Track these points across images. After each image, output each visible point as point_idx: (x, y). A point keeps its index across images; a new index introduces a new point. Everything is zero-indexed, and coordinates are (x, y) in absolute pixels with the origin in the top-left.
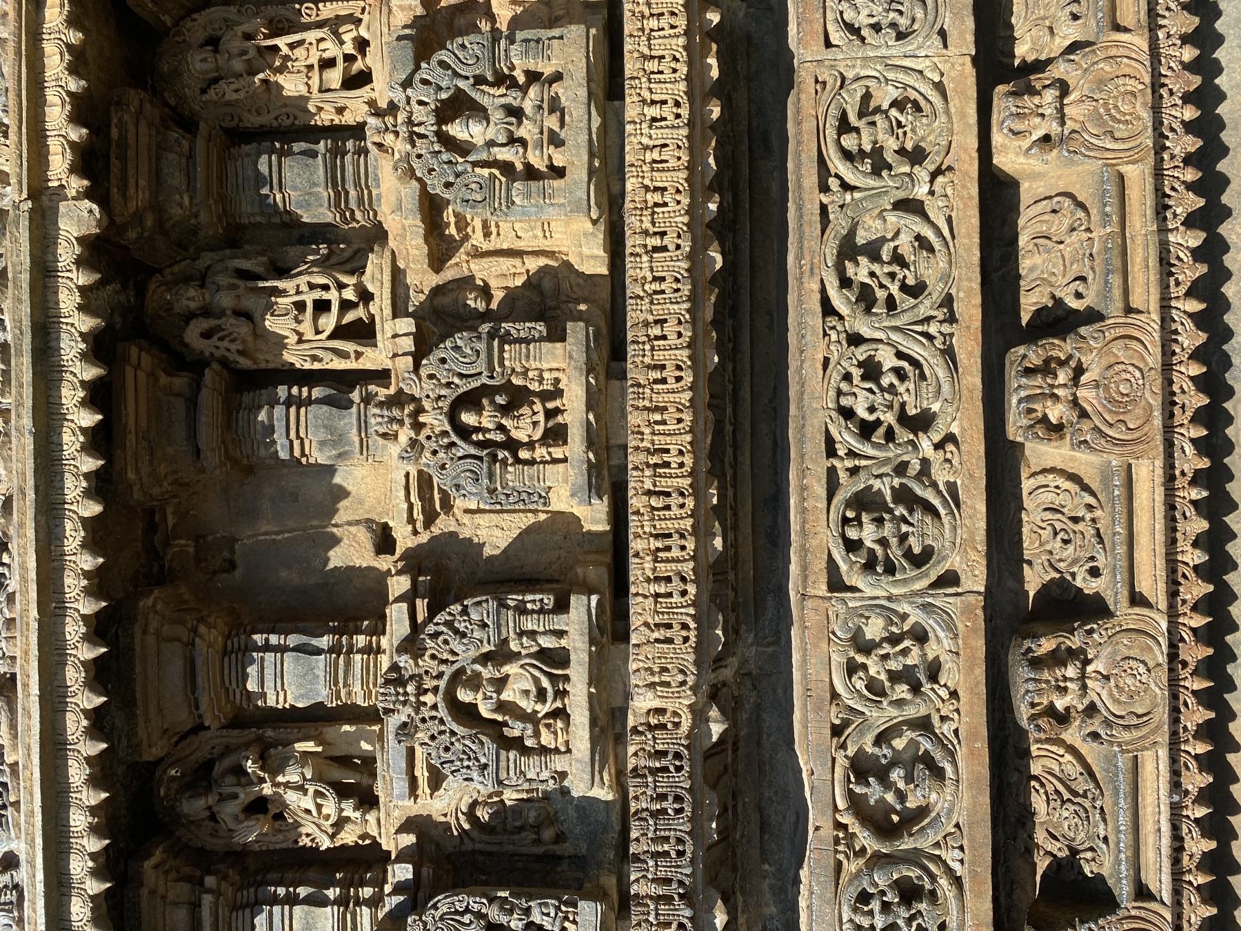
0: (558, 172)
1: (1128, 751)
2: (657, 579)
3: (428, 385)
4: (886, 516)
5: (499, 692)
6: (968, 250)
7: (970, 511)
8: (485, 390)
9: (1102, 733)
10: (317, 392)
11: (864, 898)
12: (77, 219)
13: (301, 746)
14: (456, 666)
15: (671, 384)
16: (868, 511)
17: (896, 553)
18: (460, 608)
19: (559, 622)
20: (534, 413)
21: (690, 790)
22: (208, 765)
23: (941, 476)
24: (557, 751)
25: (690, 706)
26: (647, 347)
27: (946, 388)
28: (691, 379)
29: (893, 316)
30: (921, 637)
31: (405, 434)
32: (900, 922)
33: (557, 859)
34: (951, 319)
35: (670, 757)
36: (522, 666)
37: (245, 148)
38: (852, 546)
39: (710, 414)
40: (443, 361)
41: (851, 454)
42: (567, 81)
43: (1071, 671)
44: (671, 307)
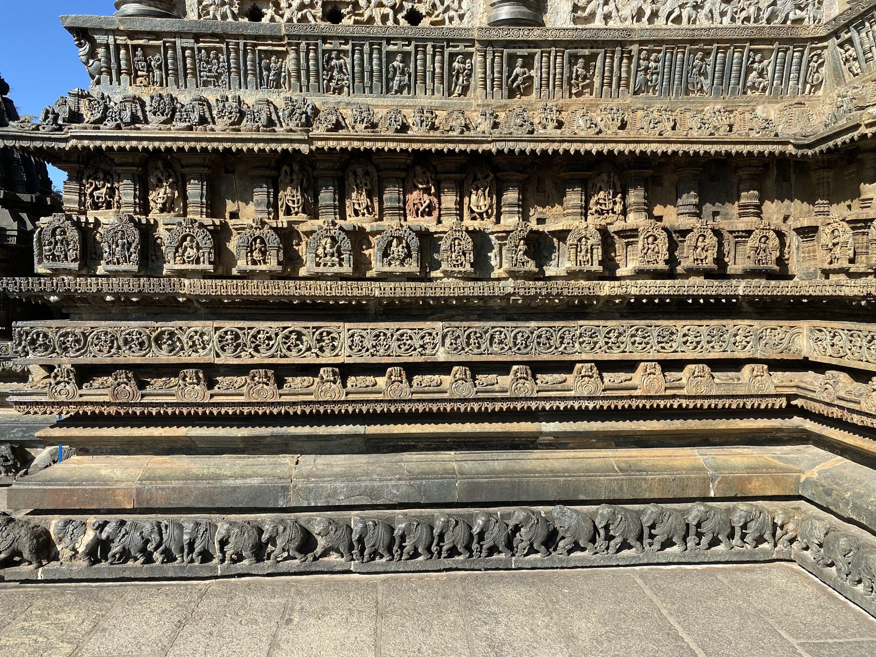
3: (266, 231)
8: (266, 245)
10: (271, 199)
11: (140, 334)
12: (304, 148)
13: (176, 193)
19: (207, 262)
22: (171, 167)
23: (243, 354)
30: (204, 348)
31: (254, 225)
33: (147, 259)
34: (281, 357)
37: (336, 183)
38: (226, 333)
43: (195, 381)
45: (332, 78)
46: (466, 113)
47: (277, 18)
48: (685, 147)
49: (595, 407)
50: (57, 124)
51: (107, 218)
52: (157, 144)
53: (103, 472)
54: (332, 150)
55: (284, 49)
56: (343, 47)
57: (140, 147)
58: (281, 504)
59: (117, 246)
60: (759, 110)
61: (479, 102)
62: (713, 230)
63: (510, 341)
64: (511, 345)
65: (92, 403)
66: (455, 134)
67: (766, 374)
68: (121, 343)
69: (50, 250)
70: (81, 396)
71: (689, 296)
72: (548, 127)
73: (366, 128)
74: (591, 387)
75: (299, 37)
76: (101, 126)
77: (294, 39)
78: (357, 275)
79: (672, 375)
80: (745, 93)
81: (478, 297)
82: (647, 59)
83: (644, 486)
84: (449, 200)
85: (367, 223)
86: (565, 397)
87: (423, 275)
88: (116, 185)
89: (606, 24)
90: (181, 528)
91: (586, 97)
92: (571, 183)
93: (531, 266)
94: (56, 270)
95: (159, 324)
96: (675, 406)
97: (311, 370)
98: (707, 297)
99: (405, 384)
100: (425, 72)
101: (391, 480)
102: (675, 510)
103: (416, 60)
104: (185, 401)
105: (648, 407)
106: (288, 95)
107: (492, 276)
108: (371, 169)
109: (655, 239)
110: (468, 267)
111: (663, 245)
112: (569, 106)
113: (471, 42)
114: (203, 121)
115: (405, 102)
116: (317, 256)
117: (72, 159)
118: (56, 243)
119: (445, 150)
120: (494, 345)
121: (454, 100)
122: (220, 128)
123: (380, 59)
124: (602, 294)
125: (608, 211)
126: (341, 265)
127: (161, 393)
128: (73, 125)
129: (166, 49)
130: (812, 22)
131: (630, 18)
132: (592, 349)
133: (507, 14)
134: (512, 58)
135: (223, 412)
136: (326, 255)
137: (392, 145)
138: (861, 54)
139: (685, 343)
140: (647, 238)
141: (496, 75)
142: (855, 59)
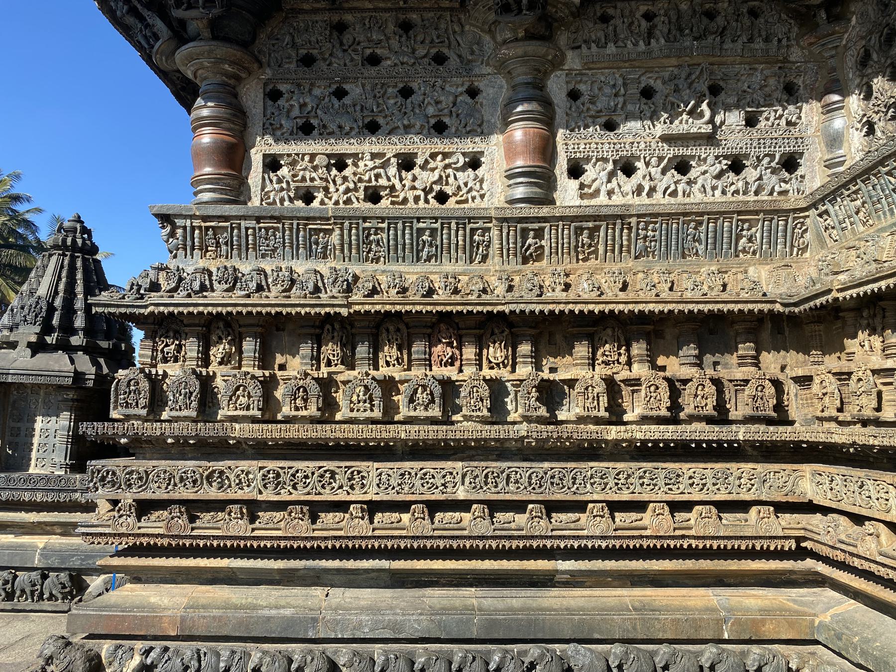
10: (315, 353)
11: (194, 472)
12: (344, 312)
17: (266, 481)
19: (256, 409)
23: (282, 491)
30: (248, 486)
31: (298, 376)
33: (205, 406)
34: (316, 494)
38: (268, 472)
45: (370, 250)
46: (485, 278)
47: (326, 200)
48: (681, 307)
49: (607, 546)
50: (140, 294)
51: (174, 370)
52: (219, 309)
53: (153, 600)
54: (367, 313)
55: (331, 227)
56: (380, 225)
57: (206, 312)
58: (311, 635)
59: (180, 395)
60: (751, 270)
61: (497, 268)
62: (711, 380)
63: (524, 480)
64: (526, 484)
65: (148, 535)
66: (473, 298)
67: (773, 516)
68: (177, 481)
69: (124, 399)
70: (139, 528)
71: (692, 441)
72: (556, 290)
73: (398, 293)
74: (603, 526)
75: (343, 218)
76: (175, 295)
77: (339, 219)
78: (386, 419)
79: (680, 516)
80: (737, 256)
81: (494, 440)
82: (646, 229)
83: (658, 626)
84: (469, 352)
85: (396, 373)
86: (578, 536)
87: (445, 419)
88: (183, 342)
89: (610, 199)
90: (218, 655)
91: (592, 262)
92: (579, 338)
93: (543, 412)
94: (128, 416)
95: (211, 464)
96: (685, 547)
97: (342, 506)
98: (709, 442)
99: (427, 521)
100: (450, 244)
101: (413, 614)
102: (689, 651)
103: (442, 235)
104: (229, 534)
105: (659, 547)
106: (333, 265)
107: (509, 419)
108: (402, 327)
109: (657, 388)
110: (485, 412)
111: (664, 392)
112: (576, 270)
113: (490, 219)
114: (260, 288)
115: (432, 269)
116: (351, 402)
117: (149, 321)
118: (130, 393)
119: (465, 311)
120: (511, 485)
121: (475, 267)
122: (274, 295)
123: (412, 234)
124: (609, 438)
125: (613, 362)
126: (372, 410)
127: (209, 526)
128: (153, 294)
129: (232, 229)
130: (796, 193)
131: (631, 193)
132: (603, 489)
133: (521, 194)
134: (525, 233)
135: (262, 545)
136: (359, 402)
137: (419, 308)
138: (837, 224)
139: (691, 485)
140: (649, 387)
141: (511, 245)
142: (833, 228)
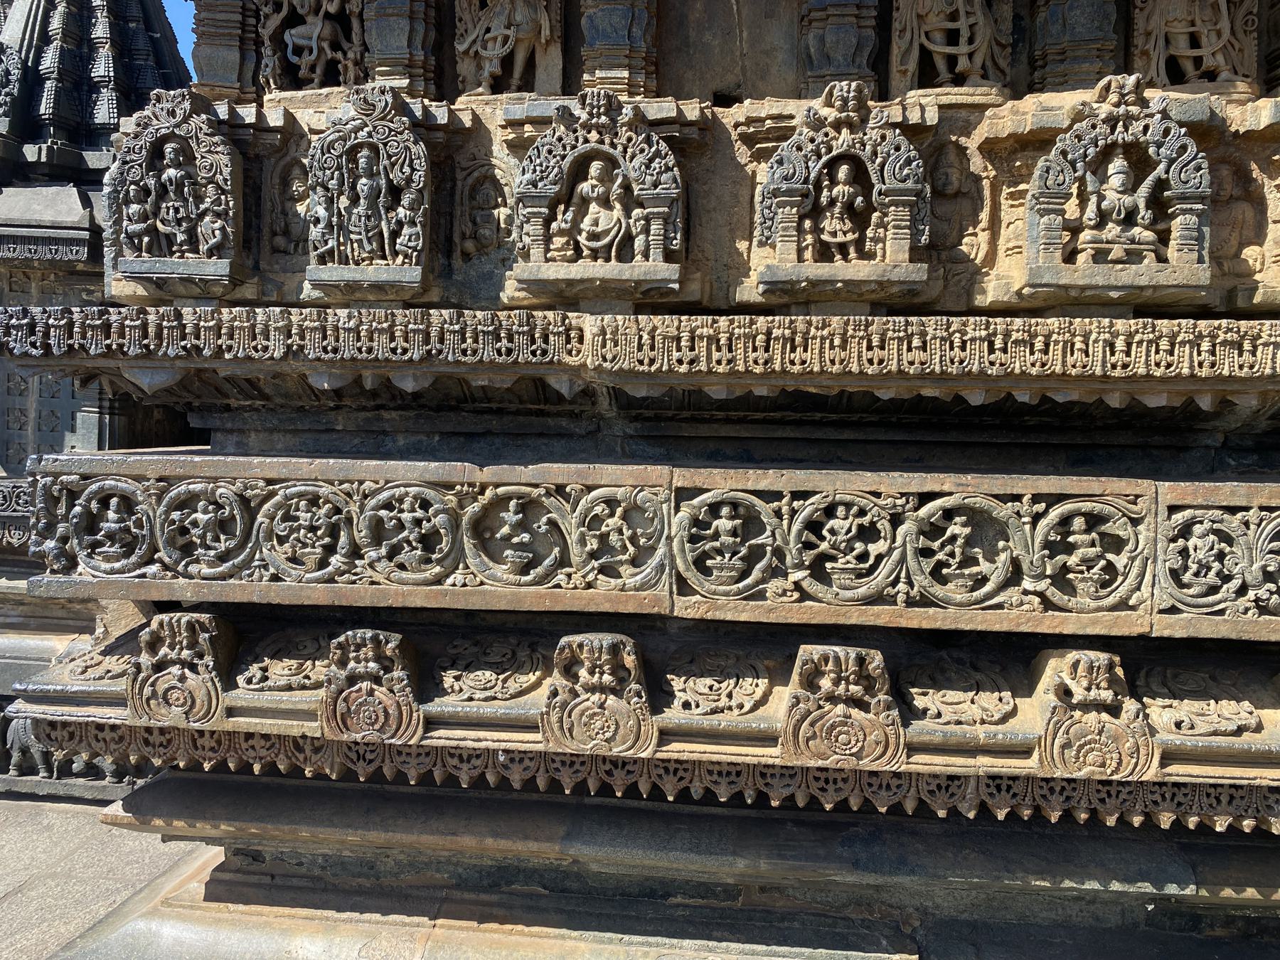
0: (1070, 257)
1: (542, 720)
2: (692, 339)
3: (874, 134)
4: (738, 540)
5: (598, 199)
6: (971, 620)
7: (740, 608)
9: (558, 698)
11: (425, 505)
14: (621, 160)
15: (866, 355)
16: (743, 524)
18: (670, 164)
19: (656, 253)
20: (845, 233)
21: (516, 362)
23: (774, 585)
24: (547, 250)
25: (584, 365)
26: (902, 334)
27: (849, 594)
28: (870, 372)
29: (915, 553)
30: (635, 562)
31: (831, 114)
32: (406, 533)
33: (449, 254)
34: (910, 603)
35: (544, 346)
36: (619, 220)
39: (835, 392)
40: (897, 149)
41: (793, 512)
42: (1155, 265)
44: (938, 356)
51: (323, 112)
59: (355, 200)
68: (362, 535)
69: (144, 217)
70: (231, 712)
94: (160, 284)
95: (488, 473)
118: (163, 192)
127: (493, 712)
